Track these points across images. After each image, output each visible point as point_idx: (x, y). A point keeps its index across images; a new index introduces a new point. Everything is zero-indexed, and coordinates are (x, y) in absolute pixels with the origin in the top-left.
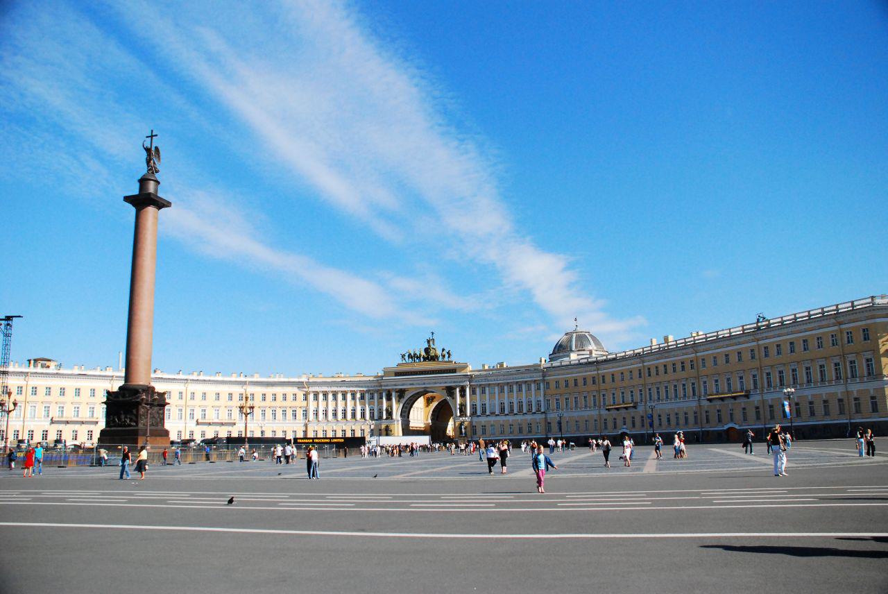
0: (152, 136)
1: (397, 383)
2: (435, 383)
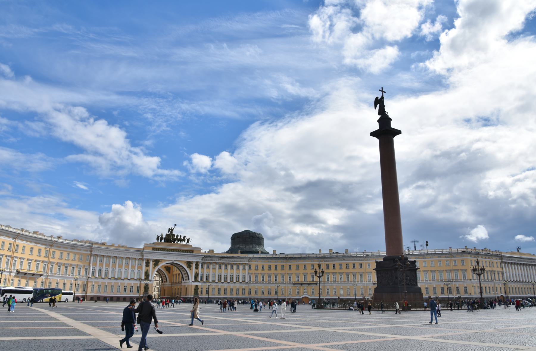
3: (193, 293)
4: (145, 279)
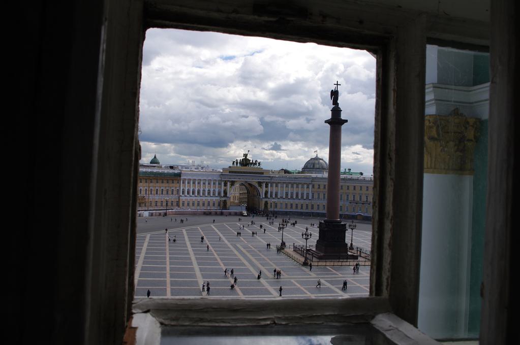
1: (231, 177)
2: (253, 179)
3: (263, 207)
4: (224, 196)
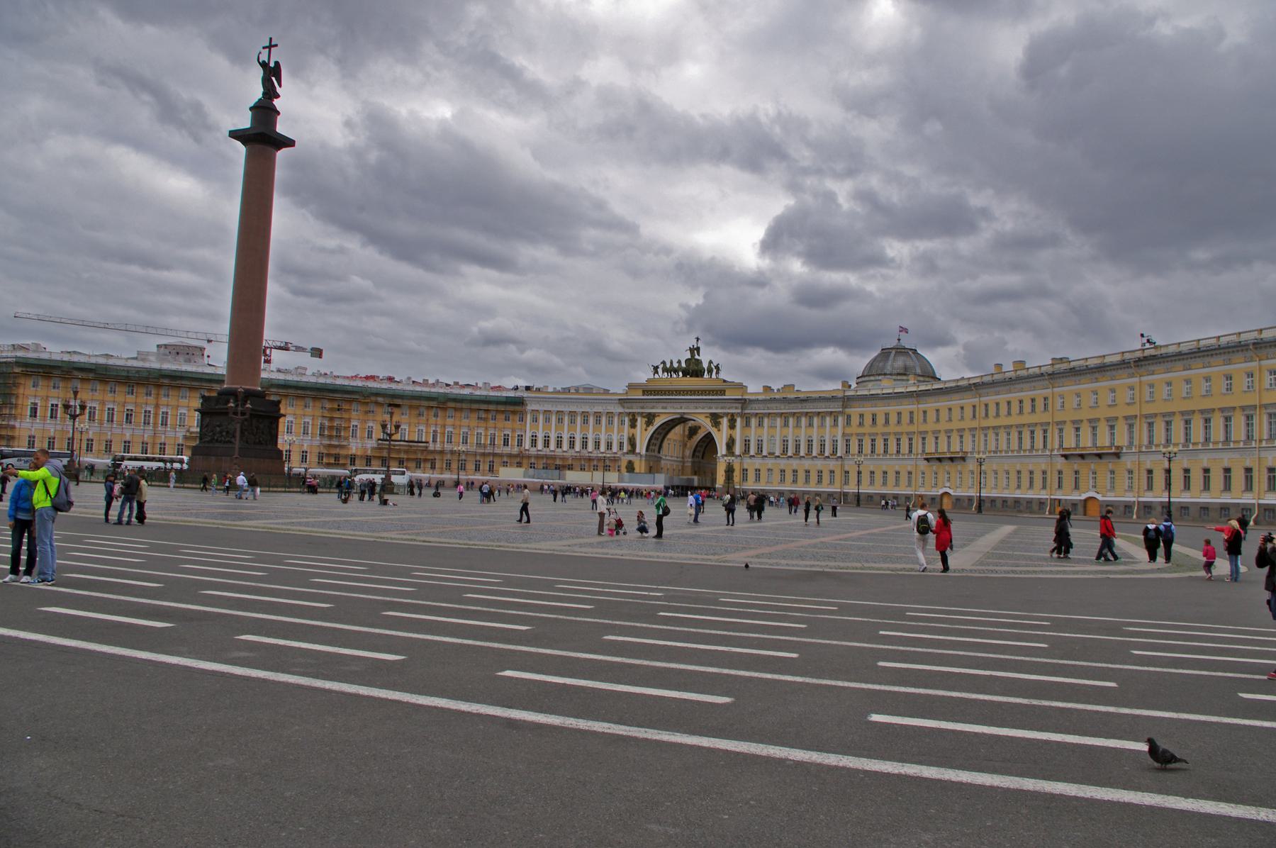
0: (270, 47)
